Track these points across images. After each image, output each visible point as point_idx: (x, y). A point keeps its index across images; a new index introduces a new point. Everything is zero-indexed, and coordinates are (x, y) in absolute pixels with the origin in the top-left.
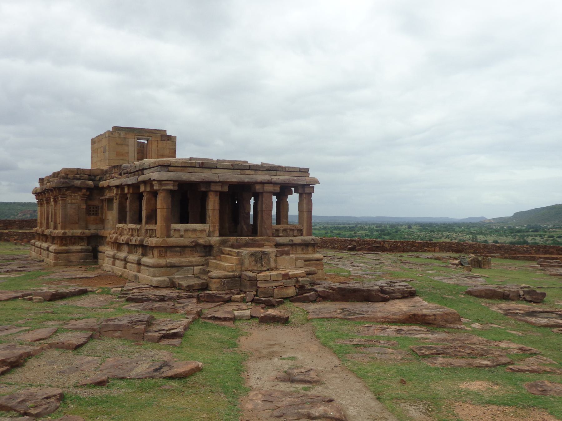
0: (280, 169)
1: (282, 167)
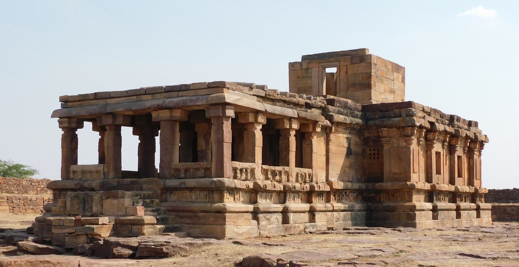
0: (183, 88)
1: (186, 85)
